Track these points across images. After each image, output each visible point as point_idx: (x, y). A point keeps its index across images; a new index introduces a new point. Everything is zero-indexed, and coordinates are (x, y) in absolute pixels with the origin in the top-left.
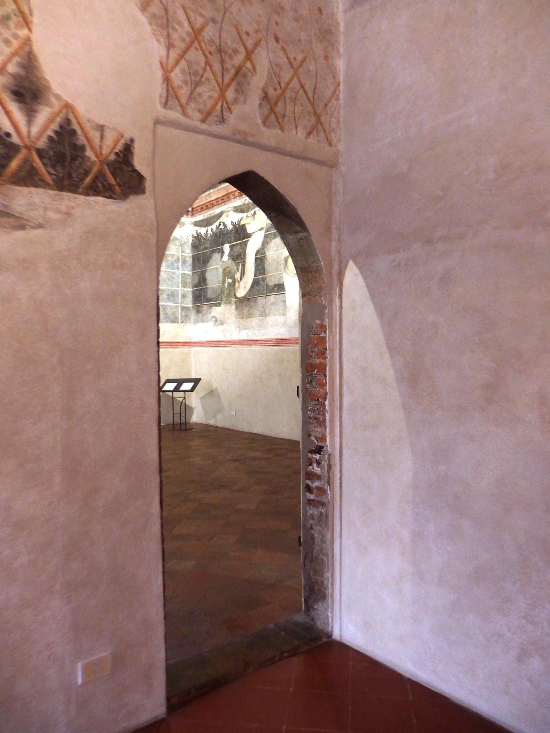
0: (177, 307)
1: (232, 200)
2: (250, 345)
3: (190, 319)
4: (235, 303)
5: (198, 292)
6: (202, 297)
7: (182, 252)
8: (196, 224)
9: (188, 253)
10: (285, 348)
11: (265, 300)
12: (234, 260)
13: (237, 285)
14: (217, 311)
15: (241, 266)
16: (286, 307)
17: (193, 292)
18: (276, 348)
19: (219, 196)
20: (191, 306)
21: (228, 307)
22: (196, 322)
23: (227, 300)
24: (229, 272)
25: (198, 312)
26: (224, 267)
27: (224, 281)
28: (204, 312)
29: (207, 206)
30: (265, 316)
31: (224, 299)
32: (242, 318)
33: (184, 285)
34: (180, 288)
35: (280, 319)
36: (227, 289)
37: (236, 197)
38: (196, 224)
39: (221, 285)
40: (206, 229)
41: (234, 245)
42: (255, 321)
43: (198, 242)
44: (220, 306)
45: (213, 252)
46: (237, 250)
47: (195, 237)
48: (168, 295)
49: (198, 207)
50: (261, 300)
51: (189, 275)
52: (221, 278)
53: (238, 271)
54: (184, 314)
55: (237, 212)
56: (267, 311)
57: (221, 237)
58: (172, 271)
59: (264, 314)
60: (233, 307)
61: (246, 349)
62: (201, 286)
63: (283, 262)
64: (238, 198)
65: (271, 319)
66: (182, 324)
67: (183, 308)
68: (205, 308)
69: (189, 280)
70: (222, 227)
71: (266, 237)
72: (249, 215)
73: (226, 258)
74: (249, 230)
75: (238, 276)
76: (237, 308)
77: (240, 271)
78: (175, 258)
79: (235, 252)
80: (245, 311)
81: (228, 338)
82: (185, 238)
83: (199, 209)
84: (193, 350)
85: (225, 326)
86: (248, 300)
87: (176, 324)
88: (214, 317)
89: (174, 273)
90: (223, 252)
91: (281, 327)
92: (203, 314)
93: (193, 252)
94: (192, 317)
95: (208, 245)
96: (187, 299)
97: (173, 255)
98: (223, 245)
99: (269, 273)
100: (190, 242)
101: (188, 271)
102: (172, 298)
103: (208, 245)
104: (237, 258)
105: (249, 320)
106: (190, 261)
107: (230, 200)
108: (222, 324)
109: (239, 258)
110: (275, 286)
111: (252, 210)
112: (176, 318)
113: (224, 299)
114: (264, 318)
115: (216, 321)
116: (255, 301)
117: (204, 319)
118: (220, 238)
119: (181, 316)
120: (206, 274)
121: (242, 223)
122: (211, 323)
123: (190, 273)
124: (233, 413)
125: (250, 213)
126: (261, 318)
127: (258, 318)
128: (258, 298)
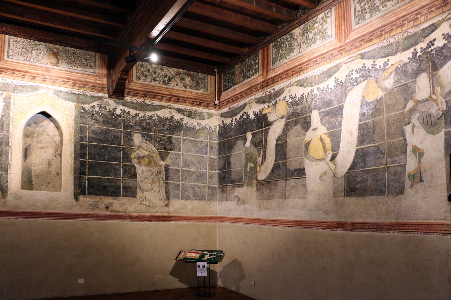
0: (204, 187)
1: (255, 93)
2: (270, 224)
3: (216, 197)
4: (257, 185)
5: (223, 174)
6: (227, 179)
7: (210, 139)
8: (222, 115)
9: (215, 140)
10: (305, 230)
11: (285, 183)
12: (256, 146)
13: (258, 169)
14: (239, 192)
15: (262, 151)
16: (306, 191)
17: (219, 174)
18: (295, 229)
19: (243, 90)
20: (216, 186)
21: (250, 189)
22: (221, 200)
23: (248, 182)
24: (251, 157)
25: (223, 191)
28: (228, 192)
29: (232, 99)
30: (285, 199)
31: (246, 181)
32: (263, 199)
33: (212, 168)
34: (207, 171)
35: (300, 202)
37: (258, 90)
38: (222, 115)
40: (231, 119)
41: (256, 133)
42: (275, 202)
43: (224, 130)
44: (242, 187)
45: (237, 139)
46: (259, 137)
47: (222, 126)
48: (197, 176)
49: (224, 101)
50: (281, 184)
51: (215, 159)
52: (243, 163)
53: (260, 156)
54: (210, 192)
55: (259, 103)
56: (287, 194)
57: (244, 126)
58: (201, 155)
59: (284, 197)
60: (255, 188)
61: (266, 228)
62: (226, 169)
63: (304, 147)
64: (260, 90)
65: (290, 202)
66: (209, 202)
67: (210, 188)
68: (229, 188)
69: (216, 164)
70: (245, 117)
71: (287, 124)
72: (270, 105)
73: (248, 144)
74: (271, 118)
75: (259, 160)
76: (258, 190)
77: (261, 156)
78: (204, 144)
79: (257, 139)
80: (265, 193)
81: (249, 216)
82: (213, 127)
83: (225, 103)
84: (218, 224)
85: (247, 206)
86: (269, 183)
87: (204, 201)
88: (236, 197)
89: (202, 157)
90: (246, 140)
91: (301, 209)
92: (227, 193)
93: (219, 139)
94: (218, 196)
95: (232, 133)
96: (214, 180)
97: (202, 142)
98: (246, 133)
99: (289, 159)
100: (217, 130)
101: (215, 156)
102: (200, 179)
103: (232, 133)
104: (258, 145)
105: (268, 201)
106: (216, 147)
107: (252, 93)
108: (244, 203)
109: (260, 144)
110: (296, 170)
111: (273, 100)
112: (204, 196)
114: (284, 200)
115: (239, 200)
116: (276, 184)
117: (228, 197)
118: (243, 127)
119: (208, 195)
120: (231, 159)
121: (264, 112)
122: (234, 202)
123: (217, 157)
124: (253, 284)
125: (271, 103)
126: (281, 200)
127: (278, 200)
128: (279, 182)
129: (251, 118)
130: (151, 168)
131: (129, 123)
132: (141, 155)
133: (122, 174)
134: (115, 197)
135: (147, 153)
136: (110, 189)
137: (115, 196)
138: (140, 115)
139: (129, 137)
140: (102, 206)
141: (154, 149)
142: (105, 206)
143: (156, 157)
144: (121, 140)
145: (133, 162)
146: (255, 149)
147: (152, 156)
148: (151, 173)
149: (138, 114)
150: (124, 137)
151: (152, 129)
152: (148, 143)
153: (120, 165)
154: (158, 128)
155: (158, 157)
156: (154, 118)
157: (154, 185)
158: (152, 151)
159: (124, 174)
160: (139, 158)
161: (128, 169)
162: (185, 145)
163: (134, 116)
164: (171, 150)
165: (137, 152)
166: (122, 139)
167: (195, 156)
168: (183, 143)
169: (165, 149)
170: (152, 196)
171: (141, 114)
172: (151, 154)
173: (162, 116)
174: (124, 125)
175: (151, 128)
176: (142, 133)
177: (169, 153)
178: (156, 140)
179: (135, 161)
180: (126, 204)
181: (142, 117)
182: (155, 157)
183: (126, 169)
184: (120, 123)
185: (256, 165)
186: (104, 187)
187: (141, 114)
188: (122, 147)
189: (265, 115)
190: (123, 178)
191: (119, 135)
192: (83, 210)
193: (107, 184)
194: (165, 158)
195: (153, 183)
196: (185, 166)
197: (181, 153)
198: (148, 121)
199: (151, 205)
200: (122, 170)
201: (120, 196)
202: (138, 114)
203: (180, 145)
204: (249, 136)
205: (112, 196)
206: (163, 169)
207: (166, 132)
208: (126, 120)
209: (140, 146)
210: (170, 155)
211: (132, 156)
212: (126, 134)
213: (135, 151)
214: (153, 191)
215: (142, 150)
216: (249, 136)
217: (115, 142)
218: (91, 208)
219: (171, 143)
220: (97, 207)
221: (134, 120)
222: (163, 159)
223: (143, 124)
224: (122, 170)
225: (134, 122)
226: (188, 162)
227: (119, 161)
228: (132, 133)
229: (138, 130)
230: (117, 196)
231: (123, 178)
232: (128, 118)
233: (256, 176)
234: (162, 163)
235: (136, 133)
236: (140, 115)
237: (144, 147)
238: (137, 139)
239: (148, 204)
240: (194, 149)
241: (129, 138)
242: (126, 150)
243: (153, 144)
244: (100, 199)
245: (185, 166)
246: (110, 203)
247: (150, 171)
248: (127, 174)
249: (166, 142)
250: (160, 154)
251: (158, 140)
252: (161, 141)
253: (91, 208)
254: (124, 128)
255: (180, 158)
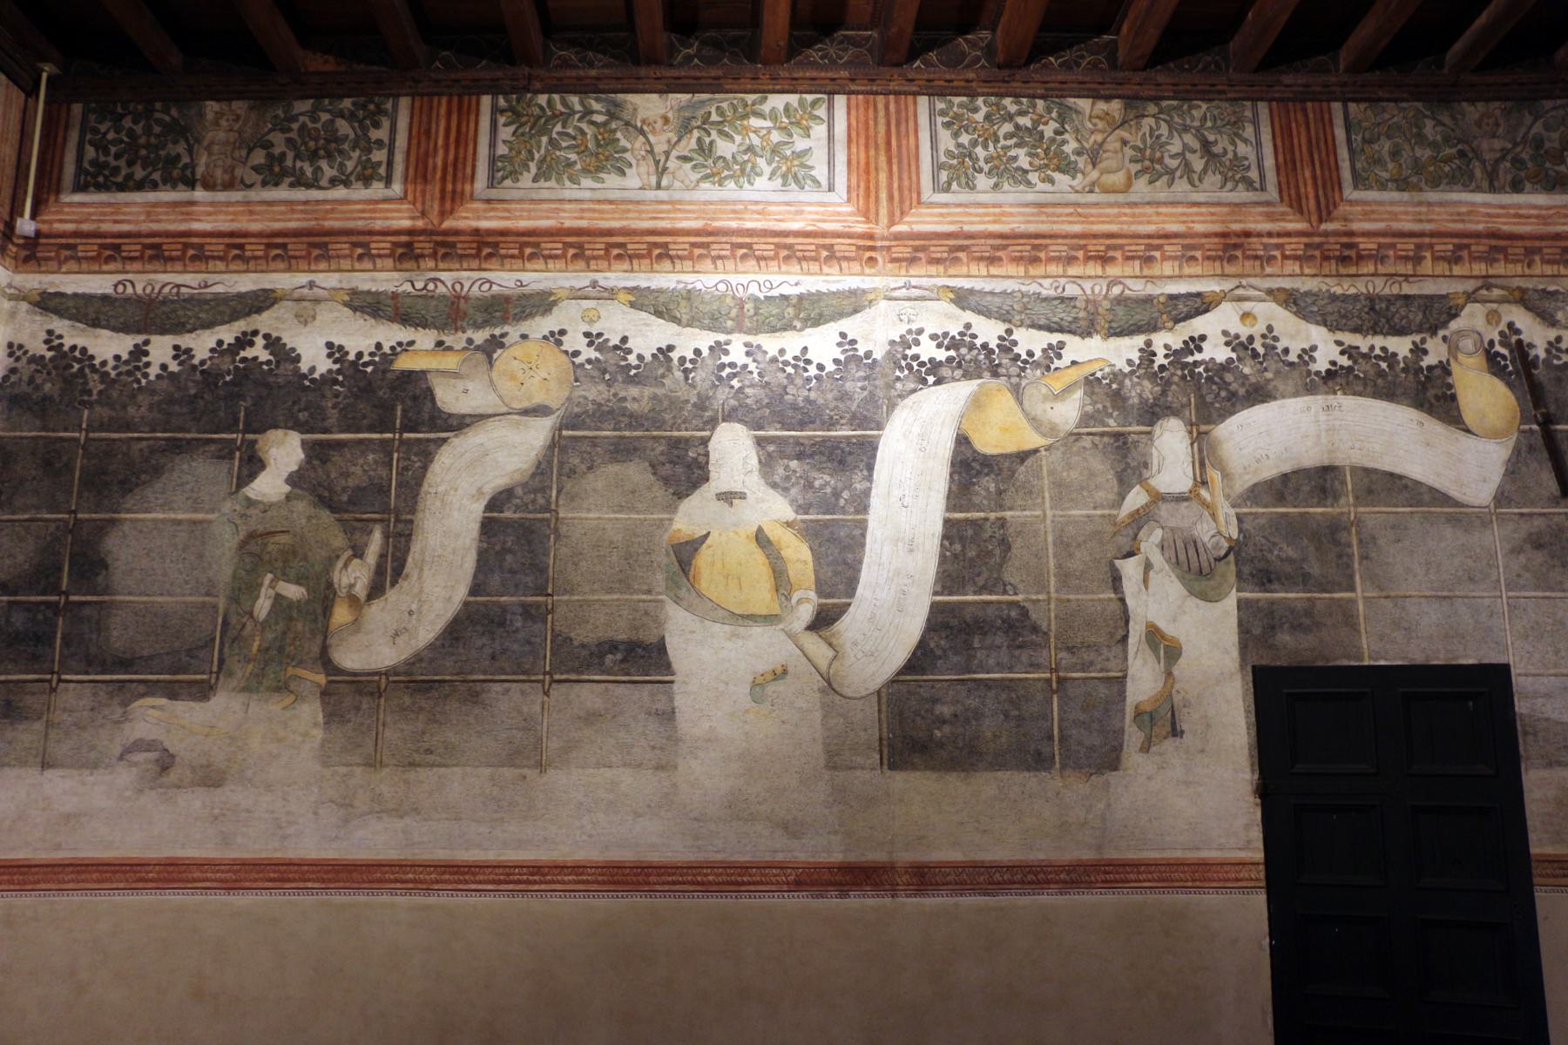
13: (341, 614)
26: (255, 524)
27: (245, 588)
36: (265, 625)
39: (222, 603)
46: (358, 470)
60: (310, 711)
75: (355, 576)
76: (333, 716)
104: (351, 502)
113: (242, 671)
129: (304, 367)
146: (326, 516)
185: (324, 597)
189: (409, 376)
204: (285, 452)
216: (285, 452)
233: (325, 649)
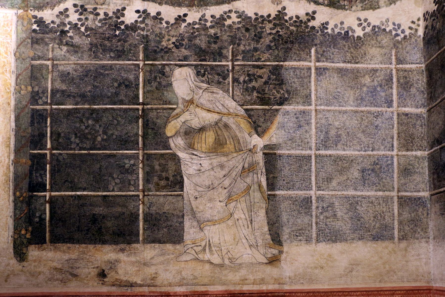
130: (224, 159)
131: (160, 42)
132: (195, 123)
133: (141, 182)
134: (123, 246)
135: (211, 118)
136: (109, 224)
137: (123, 242)
138: (189, 20)
139: (159, 80)
140: (88, 271)
141: (232, 105)
142: (96, 271)
143: (238, 126)
144: (138, 89)
145: (172, 145)
147: (226, 126)
148: (224, 173)
149: (185, 15)
150: (147, 82)
151: (224, 52)
152: (215, 89)
153: (136, 157)
154: (242, 48)
155: (244, 125)
156: (228, 22)
157: (233, 204)
158: (225, 111)
159: (147, 180)
160: (190, 133)
161: (157, 167)
162: (324, 83)
163: (172, 21)
164: (281, 104)
165: (182, 119)
166: (141, 85)
167: (356, 112)
168: (317, 80)
169: (263, 101)
170: (228, 237)
171: (193, 16)
172: (225, 119)
173: (250, 13)
174: (146, 49)
175: (221, 48)
176: (196, 66)
177: (277, 110)
178: (235, 80)
179: (177, 144)
180: (154, 262)
181: (194, 23)
182: (233, 126)
183: (152, 167)
184: (136, 46)
186: (94, 219)
187: (193, 16)
188: (140, 107)
190: (143, 191)
191: (131, 77)
192: (37, 286)
193: (99, 210)
194: (264, 126)
195: (230, 199)
196: (325, 143)
197: (313, 107)
198: (212, 31)
199: (227, 262)
200: (141, 171)
201: (137, 242)
202: (185, 15)
203: (309, 88)
205: (116, 243)
206: (260, 158)
207: (266, 56)
208: (152, 37)
209: (191, 102)
210: (279, 118)
211: (170, 131)
212: (150, 71)
213: (178, 116)
214: (230, 222)
215: (198, 110)
217: (122, 97)
218: (59, 276)
219: (281, 82)
220: (75, 276)
221: (172, 33)
222: (259, 129)
223: (197, 41)
224: (141, 171)
225: (174, 40)
226: (333, 133)
227: (135, 145)
228: (167, 69)
229: (186, 58)
230: (129, 243)
231: (143, 191)
232: (157, 31)
234: (258, 142)
235: (180, 66)
236: (189, 20)
237: (202, 101)
238: (183, 81)
239: (216, 260)
240: (350, 95)
241: (160, 83)
242: (152, 115)
243: (227, 91)
244: (84, 253)
245: (325, 143)
246: (110, 262)
247: (222, 166)
248: (156, 179)
249: (266, 83)
250: (250, 116)
251: (241, 79)
252: (250, 81)
253: (59, 276)
254: (147, 58)
255: (309, 124)
